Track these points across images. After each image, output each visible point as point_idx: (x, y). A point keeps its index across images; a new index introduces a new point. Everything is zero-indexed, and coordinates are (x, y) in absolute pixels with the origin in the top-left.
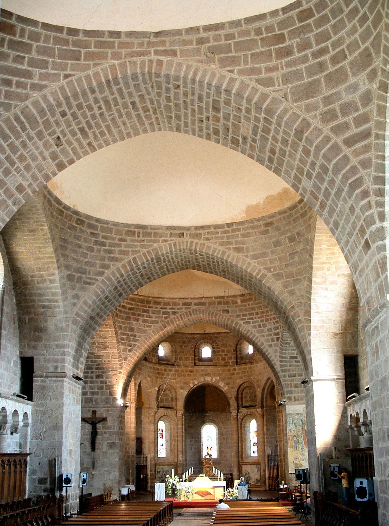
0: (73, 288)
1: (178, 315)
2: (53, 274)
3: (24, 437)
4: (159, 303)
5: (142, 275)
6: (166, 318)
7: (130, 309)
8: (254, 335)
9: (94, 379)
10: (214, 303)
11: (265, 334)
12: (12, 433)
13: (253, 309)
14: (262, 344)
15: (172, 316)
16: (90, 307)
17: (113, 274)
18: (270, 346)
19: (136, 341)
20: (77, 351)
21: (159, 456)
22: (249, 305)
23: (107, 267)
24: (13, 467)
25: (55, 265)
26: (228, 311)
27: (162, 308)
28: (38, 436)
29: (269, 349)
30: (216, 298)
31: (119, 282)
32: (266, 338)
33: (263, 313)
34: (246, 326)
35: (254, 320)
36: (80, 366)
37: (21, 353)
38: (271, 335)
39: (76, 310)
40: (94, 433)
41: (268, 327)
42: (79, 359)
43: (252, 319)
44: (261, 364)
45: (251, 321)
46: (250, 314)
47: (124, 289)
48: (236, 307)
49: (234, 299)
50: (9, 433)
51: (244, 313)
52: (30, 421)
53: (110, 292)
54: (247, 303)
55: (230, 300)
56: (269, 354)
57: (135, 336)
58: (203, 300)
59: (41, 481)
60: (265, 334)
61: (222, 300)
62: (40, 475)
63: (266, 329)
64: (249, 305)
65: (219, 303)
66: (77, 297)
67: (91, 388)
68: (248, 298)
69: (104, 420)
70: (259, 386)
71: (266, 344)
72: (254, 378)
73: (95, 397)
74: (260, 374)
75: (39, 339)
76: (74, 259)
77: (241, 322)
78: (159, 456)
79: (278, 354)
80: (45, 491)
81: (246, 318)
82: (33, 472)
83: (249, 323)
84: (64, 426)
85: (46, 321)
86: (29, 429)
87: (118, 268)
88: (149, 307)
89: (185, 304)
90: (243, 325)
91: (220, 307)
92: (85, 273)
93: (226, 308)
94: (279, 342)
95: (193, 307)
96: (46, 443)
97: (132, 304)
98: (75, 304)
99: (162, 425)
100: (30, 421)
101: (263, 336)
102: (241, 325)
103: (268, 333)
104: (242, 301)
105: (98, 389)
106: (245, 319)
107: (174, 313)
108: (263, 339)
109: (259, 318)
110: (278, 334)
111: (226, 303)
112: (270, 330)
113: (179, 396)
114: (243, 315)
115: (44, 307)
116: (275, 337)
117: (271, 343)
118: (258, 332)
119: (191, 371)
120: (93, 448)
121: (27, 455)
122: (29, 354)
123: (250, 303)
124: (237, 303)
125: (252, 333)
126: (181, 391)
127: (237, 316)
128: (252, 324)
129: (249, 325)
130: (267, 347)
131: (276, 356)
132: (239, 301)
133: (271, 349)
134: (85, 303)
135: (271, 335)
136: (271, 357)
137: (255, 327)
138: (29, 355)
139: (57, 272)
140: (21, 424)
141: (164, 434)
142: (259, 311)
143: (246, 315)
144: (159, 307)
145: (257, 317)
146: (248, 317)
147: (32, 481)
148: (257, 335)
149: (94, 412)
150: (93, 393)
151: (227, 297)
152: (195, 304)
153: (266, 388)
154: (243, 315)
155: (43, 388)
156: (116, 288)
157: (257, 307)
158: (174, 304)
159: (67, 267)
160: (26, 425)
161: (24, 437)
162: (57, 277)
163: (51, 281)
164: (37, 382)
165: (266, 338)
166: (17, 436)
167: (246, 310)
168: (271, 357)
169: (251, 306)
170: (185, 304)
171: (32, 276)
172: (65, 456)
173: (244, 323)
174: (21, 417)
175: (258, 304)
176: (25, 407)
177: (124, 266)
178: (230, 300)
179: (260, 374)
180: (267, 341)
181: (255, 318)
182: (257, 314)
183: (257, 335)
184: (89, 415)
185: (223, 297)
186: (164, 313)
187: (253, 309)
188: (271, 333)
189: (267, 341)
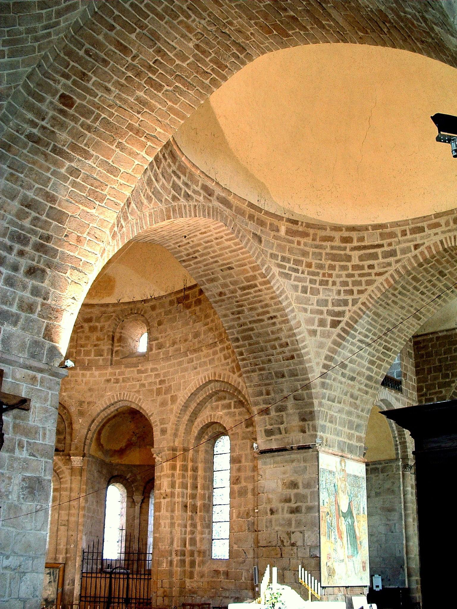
1: (191, 203)
8: (290, 304)
9: (20, 275)
10: (243, 214)
11: (309, 307)
13: (305, 254)
14: (299, 325)
15: (183, 201)
18: (313, 333)
22: (299, 243)
26: (260, 241)
29: (308, 337)
30: (251, 205)
32: (309, 315)
33: (321, 267)
34: (282, 280)
35: (300, 275)
38: (321, 313)
41: (321, 296)
43: (297, 271)
44: (97, 373)
45: (294, 274)
48: (275, 237)
49: (276, 222)
51: (287, 255)
54: (296, 239)
55: (269, 220)
56: (304, 347)
58: (230, 198)
60: (309, 307)
61: (257, 214)
63: (314, 299)
64: (299, 243)
65: (251, 217)
68: (301, 229)
69: (22, 404)
70: (81, 414)
71: (304, 327)
72: (70, 397)
74: (90, 390)
77: (275, 270)
79: (325, 352)
81: (288, 265)
83: (287, 276)
89: (205, 188)
90: (277, 277)
91: (252, 226)
93: (259, 233)
94: (338, 330)
101: (305, 310)
102: (273, 276)
103: (315, 307)
104: (288, 232)
105: (20, 307)
106: (284, 267)
108: (302, 317)
109: (309, 274)
110: (341, 314)
111: (262, 223)
112: (325, 303)
114: (283, 259)
116: (329, 319)
117: (315, 327)
118: (299, 300)
123: (303, 240)
124: (278, 230)
125: (287, 298)
128: (292, 282)
129: (286, 281)
130: (306, 334)
131: (318, 354)
132: (283, 229)
133: (313, 338)
135: (321, 313)
136: (308, 353)
137: (296, 288)
142: (314, 262)
143: (289, 261)
145: (307, 270)
146: (291, 265)
148: (294, 305)
151: (267, 213)
153: (99, 419)
154: (283, 259)
157: (314, 253)
158: (191, 176)
165: (309, 315)
167: (290, 251)
168: (308, 353)
169: (302, 247)
173: (281, 274)
175: (317, 247)
178: (269, 220)
179: (90, 390)
180: (310, 321)
181: (303, 273)
182: (309, 265)
185: (260, 210)
187: (305, 254)
188: (325, 309)
189: (310, 321)
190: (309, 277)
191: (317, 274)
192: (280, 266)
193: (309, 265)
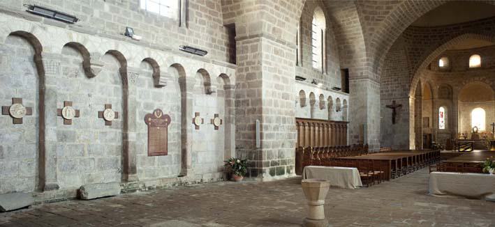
0: (369, 24)
2: (355, 18)
3: (345, 113)
5: (416, 10)
12: (337, 111)
16: (381, 35)
17: (396, 12)
20: (375, 63)
21: (440, 128)
23: (391, 8)
24: (338, 129)
25: (356, 12)
28: (353, 113)
31: (400, 17)
36: (378, 72)
37: (341, 67)
39: (372, 38)
40: (394, 114)
42: (377, 68)
47: (404, 21)
50: (335, 110)
52: (348, 104)
53: (394, 24)
59: (356, 137)
62: (355, 134)
66: (372, 29)
67: (391, 87)
69: (400, 106)
73: (394, 93)
75: (351, 57)
76: (368, 6)
78: (440, 128)
80: (358, 142)
82: (351, 132)
84: (368, 105)
85: (354, 46)
86: (348, 109)
87: (398, 8)
89: (454, 28)
92: (376, 14)
96: (358, 116)
98: (371, 34)
99: (442, 110)
100: (348, 104)
113: (454, 91)
115: (352, 38)
119: (463, 74)
120: (394, 121)
121: (347, 123)
122: (345, 66)
134: (378, 32)
138: (345, 68)
139: (357, 16)
140: (342, 106)
141: (444, 114)
147: (351, 137)
149: (394, 102)
150: (393, 90)
155: (355, 85)
156: (398, 21)
159: (364, 12)
160: (345, 107)
161: (345, 113)
162: (358, 19)
163: (355, 22)
164: (351, 82)
166: (341, 113)
170: (454, 28)
171: (343, 21)
172: (369, 123)
174: (342, 102)
176: (343, 97)
177: (402, 6)
184: (391, 103)
186: (440, 36)
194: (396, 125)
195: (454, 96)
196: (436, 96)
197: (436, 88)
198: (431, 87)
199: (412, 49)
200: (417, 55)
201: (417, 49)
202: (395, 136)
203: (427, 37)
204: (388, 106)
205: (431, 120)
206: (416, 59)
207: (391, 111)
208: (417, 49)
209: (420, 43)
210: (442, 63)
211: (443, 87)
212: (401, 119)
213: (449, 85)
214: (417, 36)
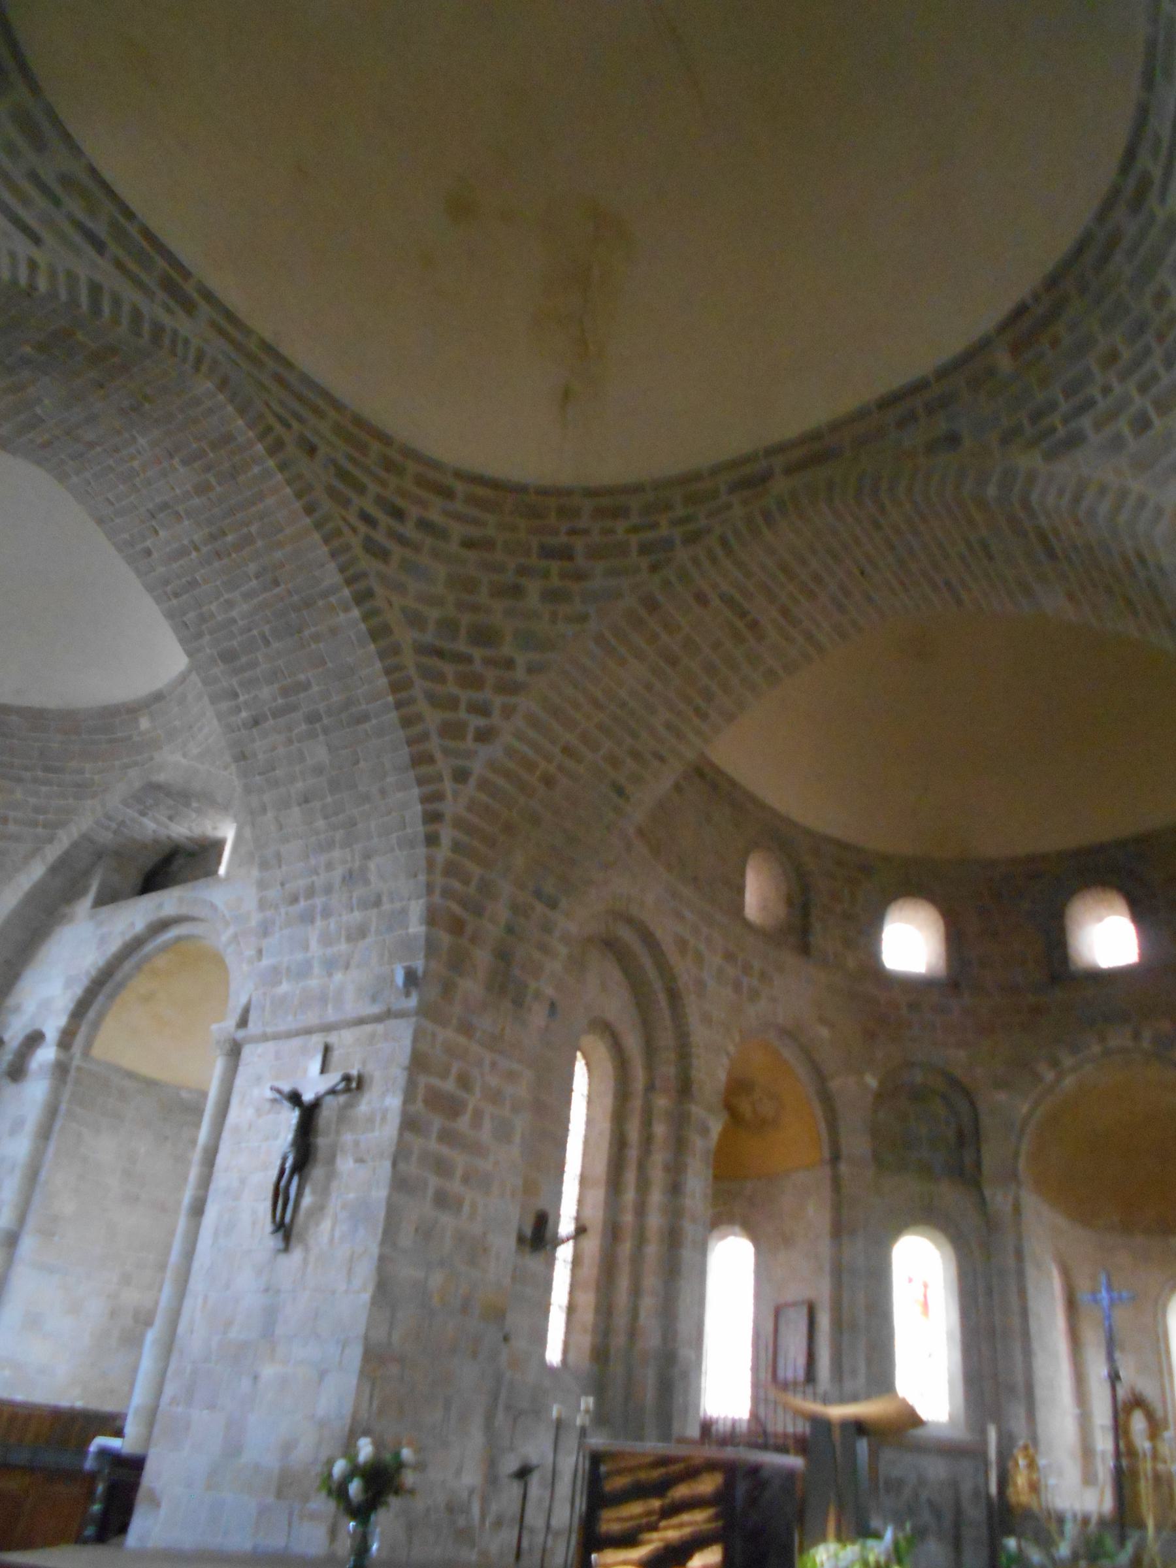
4: (620, 512)
6: (654, 568)
7: (468, 544)
15: (682, 555)
19: (513, 688)
27: (635, 529)
43: (1090, 403)
46: (1070, 390)
57: (509, 664)
65: (908, 420)
83: (1074, 441)
88: (573, 532)
95: (781, 485)
97: (476, 522)
104: (1015, 350)
105: (349, 939)
107: (692, 539)
109: (1123, 377)
113: (986, 1120)
114: (1036, 416)
124: (991, 372)
126: (1001, 1097)
127: (1006, 439)
128: (1095, 439)
132: (1004, 362)
137: (1116, 444)
144: (621, 526)
148: (1136, 486)
152: (789, 471)
183: (1136, 486)
186: (644, 549)
190: (1131, 386)
191: (1147, 352)
192: (1033, 443)
193: (1112, 357)
194: (297, 1254)
195: (991, 1156)
196: (857, 1144)
197: (858, 1087)
198: (820, 1077)
199: (448, 627)
200: (491, 675)
201: (484, 636)
202: (268, 1371)
203: (566, 554)
204: (295, 1098)
205: (824, 1321)
206: (483, 710)
207: (292, 1117)
208: (484, 636)
209: (517, 591)
210: (910, 943)
211: (918, 1095)
212: (335, 1203)
213: (954, 1083)
214: (487, 544)
